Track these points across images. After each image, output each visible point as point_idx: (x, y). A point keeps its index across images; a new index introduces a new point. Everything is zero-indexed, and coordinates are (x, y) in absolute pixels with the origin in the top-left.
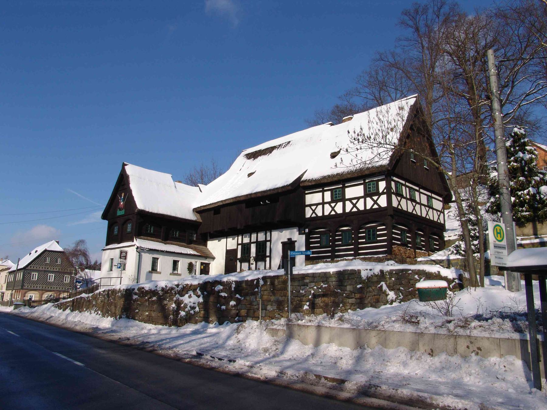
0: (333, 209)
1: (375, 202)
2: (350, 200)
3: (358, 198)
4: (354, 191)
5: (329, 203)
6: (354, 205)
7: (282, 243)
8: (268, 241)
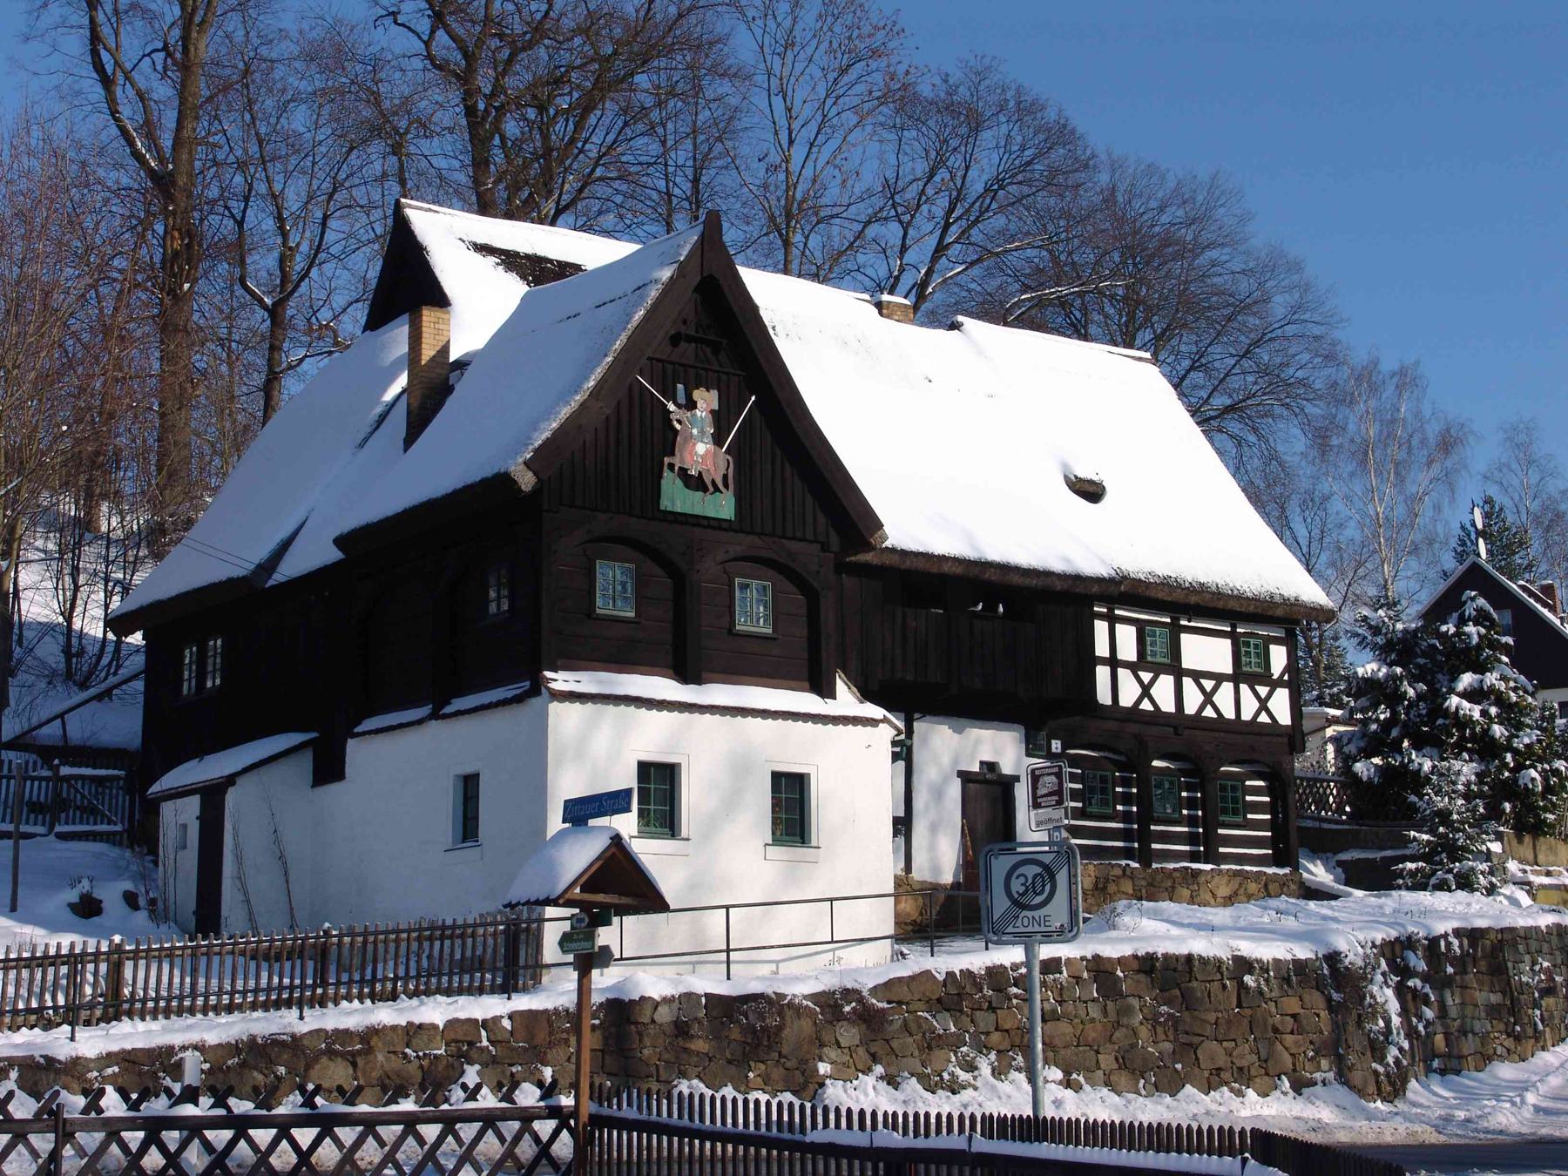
0: (1146, 691)
1: (1263, 705)
2: (1197, 676)
3: (1219, 678)
4: (1206, 651)
5: (1133, 667)
6: (1208, 698)
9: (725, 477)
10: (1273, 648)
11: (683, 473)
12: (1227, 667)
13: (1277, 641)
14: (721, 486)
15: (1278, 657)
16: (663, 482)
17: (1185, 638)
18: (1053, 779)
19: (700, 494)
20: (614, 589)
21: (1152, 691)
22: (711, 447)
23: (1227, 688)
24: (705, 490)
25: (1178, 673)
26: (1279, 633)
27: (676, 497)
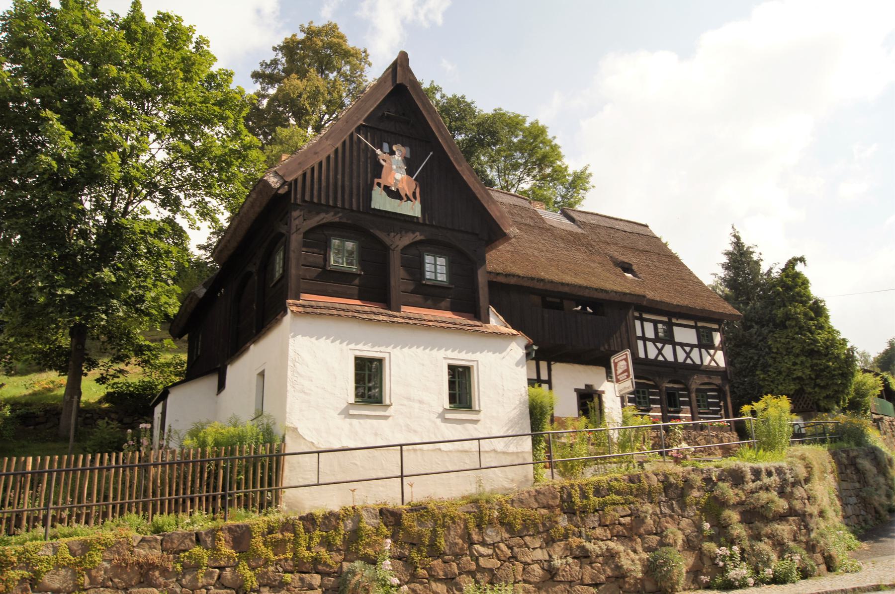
0: (660, 352)
2: (682, 345)
3: (692, 346)
4: (685, 335)
5: (654, 341)
6: (688, 355)
7: (576, 390)
8: (545, 382)
9: (414, 194)
10: (714, 333)
11: (387, 189)
12: (695, 342)
13: (717, 330)
14: (412, 198)
15: (717, 338)
16: (373, 192)
17: (675, 329)
18: (624, 363)
19: (398, 201)
20: (342, 255)
21: (663, 352)
22: (405, 176)
23: (696, 350)
24: (401, 198)
25: (674, 344)
26: (716, 327)
27: (380, 201)
